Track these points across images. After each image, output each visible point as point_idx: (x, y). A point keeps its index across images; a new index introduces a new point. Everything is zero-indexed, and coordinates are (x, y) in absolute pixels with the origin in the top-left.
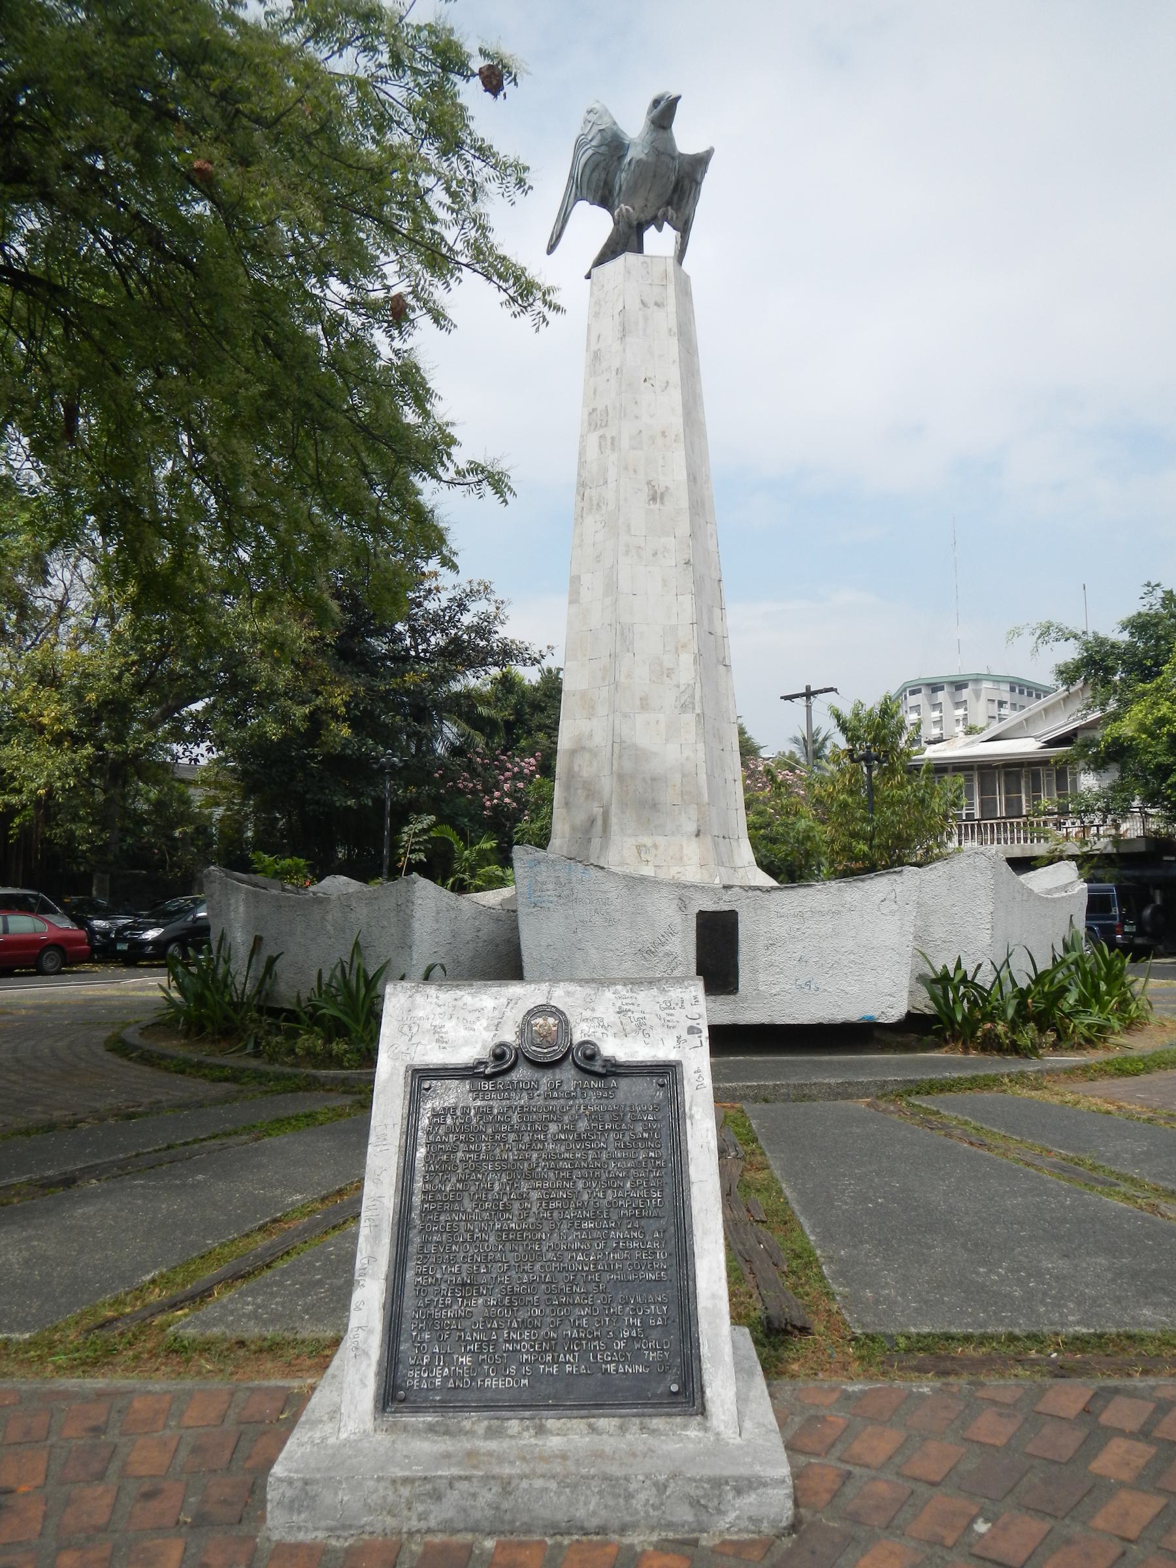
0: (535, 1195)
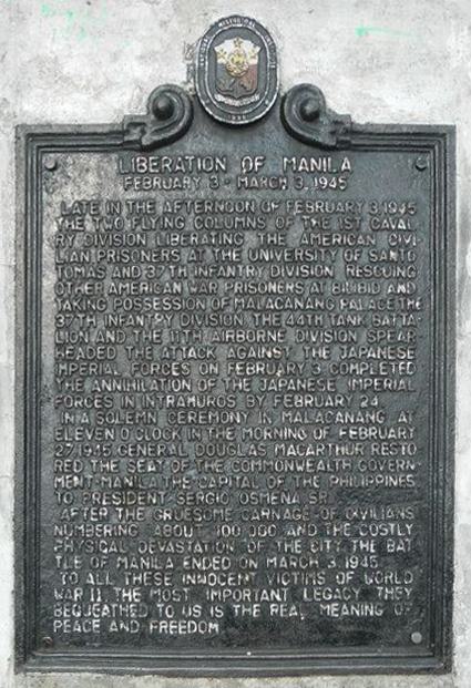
0: (224, 352)
